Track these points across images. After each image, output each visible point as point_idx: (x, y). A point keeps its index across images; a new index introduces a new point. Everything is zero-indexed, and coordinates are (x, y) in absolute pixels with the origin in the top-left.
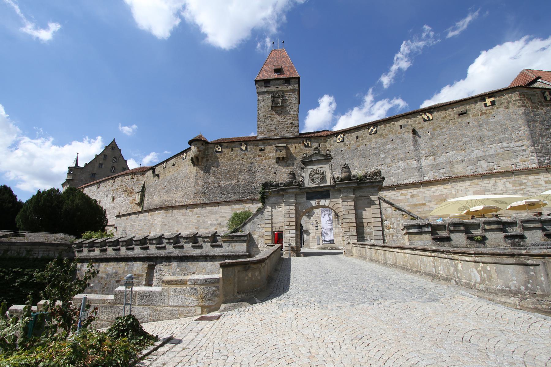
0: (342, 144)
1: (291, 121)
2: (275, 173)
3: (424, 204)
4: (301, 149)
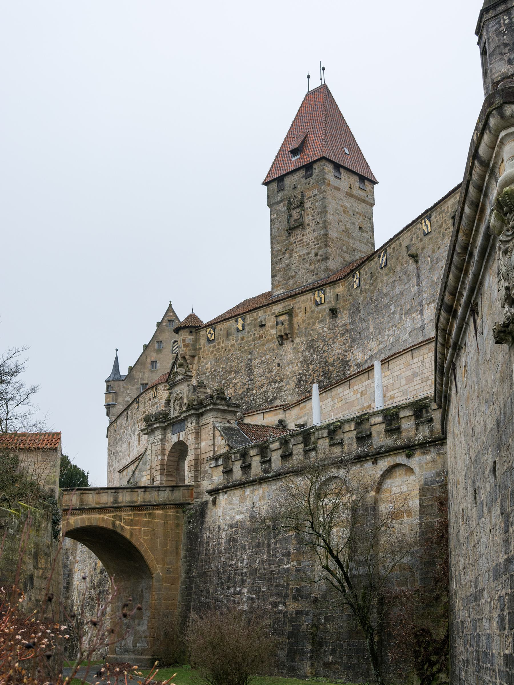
1: (316, 250)
2: (279, 365)
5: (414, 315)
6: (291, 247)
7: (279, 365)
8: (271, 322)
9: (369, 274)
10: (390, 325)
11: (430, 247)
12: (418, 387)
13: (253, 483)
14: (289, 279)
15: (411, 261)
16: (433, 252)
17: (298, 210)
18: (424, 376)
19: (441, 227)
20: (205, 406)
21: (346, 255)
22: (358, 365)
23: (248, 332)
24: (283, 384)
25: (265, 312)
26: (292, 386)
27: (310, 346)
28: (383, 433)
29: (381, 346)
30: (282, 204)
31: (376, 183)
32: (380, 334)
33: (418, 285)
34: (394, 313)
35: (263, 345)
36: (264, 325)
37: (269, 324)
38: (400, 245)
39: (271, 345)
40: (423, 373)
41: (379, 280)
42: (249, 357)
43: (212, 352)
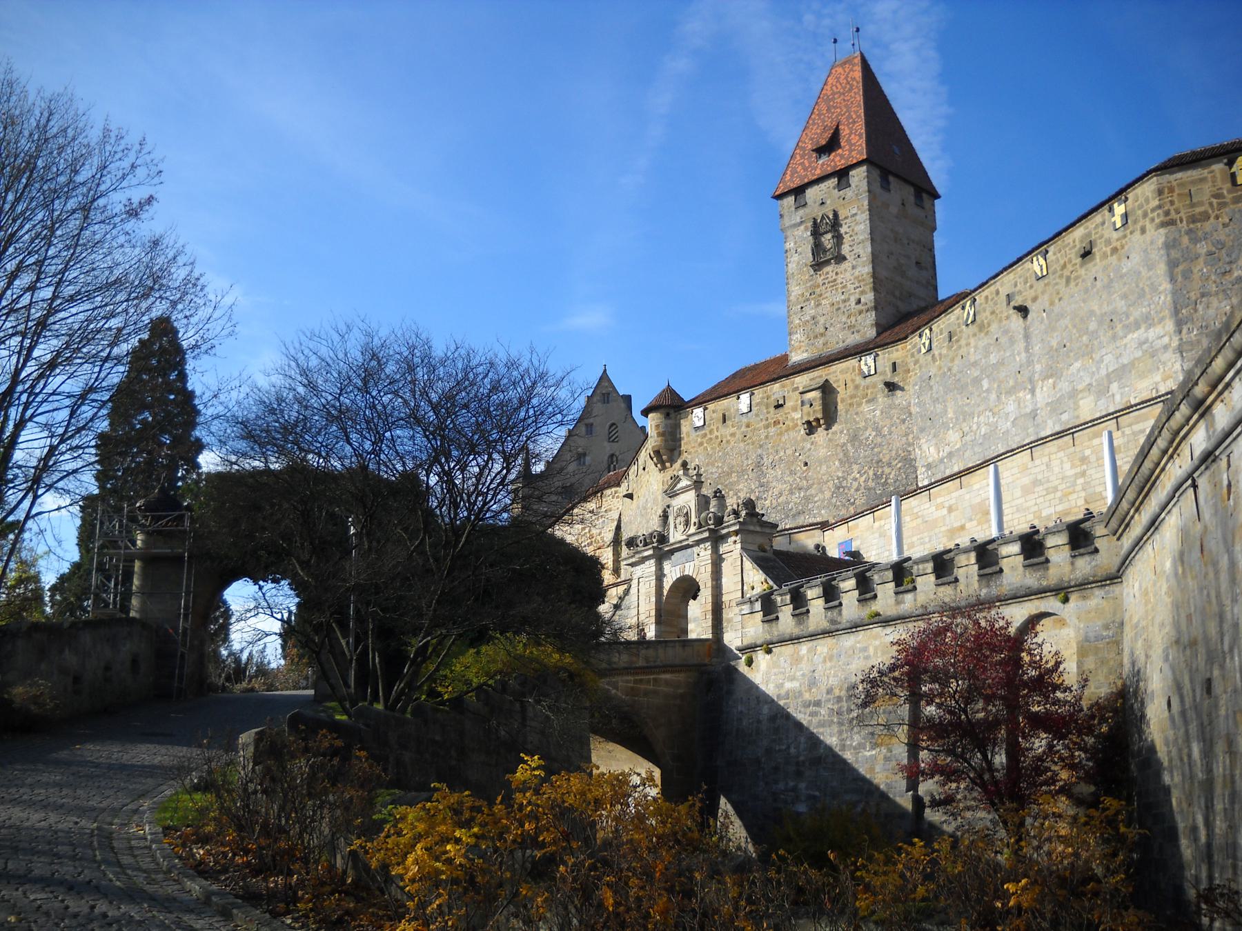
0: (929, 357)
1: (857, 296)
3: (963, 528)
4: (857, 387)
5: (1021, 394)
6: (818, 291)
7: (806, 464)
8: (793, 400)
9: (946, 334)
10: (981, 408)
11: (1046, 297)
12: (1041, 499)
13: (813, 636)
14: (816, 337)
15: (1016, 318)
16: (1052, 303)
17: (829, 236)
18: (1050, 485)
19: (1064, 267)
20: (728, 527)
21: (899, 303)
22: (929, 466)
23: (757, 415)
24: (812, 491)
25: (783, 387)
26: (828, 494)
27: (854, 438)
28: (1021, 569)
29: (968, 438)
30: (802, 227)
31: (937, 196)
32: (964, 420)
33: (1027, 350)
34: (988, 391)
35: (781, 434)
36: (781, 406)
37: (789, 404)
38: (998, 293)
39: (792, 434)
40: (1048, 481)
41: (963, 342)
42: (759, 451)
43: (701, 444)
